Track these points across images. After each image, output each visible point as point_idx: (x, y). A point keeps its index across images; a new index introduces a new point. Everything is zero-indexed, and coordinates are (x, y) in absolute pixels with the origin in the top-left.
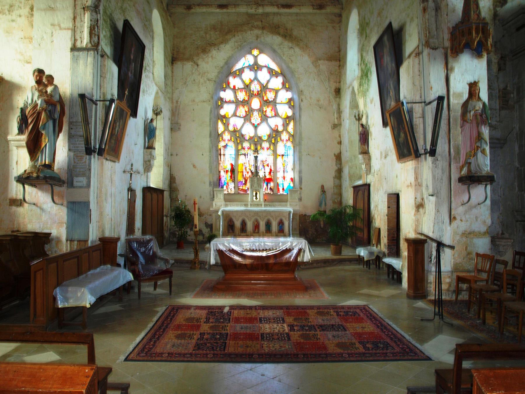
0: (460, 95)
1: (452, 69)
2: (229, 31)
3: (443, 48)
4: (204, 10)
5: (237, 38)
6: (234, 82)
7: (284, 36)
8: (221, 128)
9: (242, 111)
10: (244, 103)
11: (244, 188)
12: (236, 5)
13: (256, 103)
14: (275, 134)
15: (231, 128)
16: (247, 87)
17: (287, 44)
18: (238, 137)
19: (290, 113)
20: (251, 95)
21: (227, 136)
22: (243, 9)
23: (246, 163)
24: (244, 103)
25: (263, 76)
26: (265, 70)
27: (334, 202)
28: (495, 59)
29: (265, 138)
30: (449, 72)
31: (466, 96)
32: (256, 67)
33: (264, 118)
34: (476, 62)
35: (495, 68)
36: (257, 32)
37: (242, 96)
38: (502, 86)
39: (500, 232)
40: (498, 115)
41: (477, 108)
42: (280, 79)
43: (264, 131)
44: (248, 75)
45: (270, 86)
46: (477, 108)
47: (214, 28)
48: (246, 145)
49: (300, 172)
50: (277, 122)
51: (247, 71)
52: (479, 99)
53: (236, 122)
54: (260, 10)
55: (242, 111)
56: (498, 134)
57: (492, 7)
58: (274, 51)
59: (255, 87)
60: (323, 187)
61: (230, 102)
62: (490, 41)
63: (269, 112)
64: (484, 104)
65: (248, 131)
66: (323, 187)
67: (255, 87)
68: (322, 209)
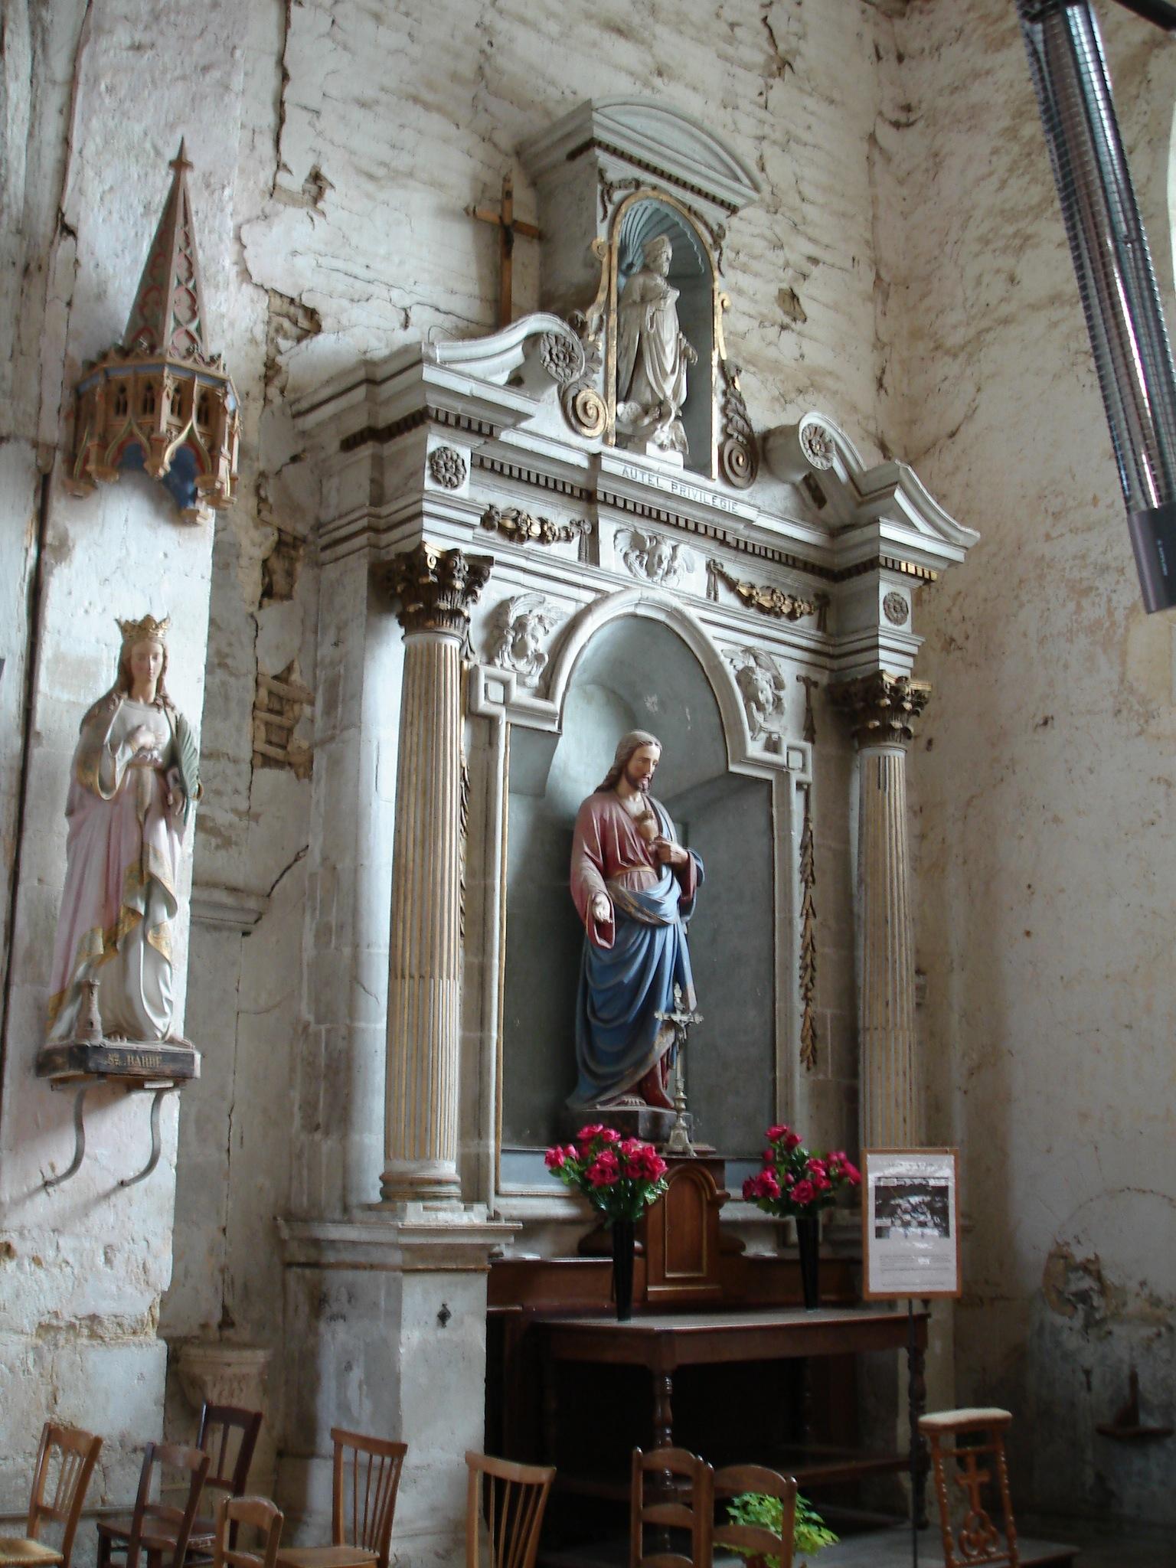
0: (84, 669)
1: (63, 550)
3: (35, 445)
28: (255, 544)
30: (47, 556)
31: (108, 677)
34: (168, 536)
35: (250, 582)
38: (272, 665)
39: (218, 1316)
40: (243, 787)
41: (145, 739)
46: (145, 739)
52: (162, 702)
56: (240, 868)
57: (260, 331)
62: (227, 465)
64: (179, 730)
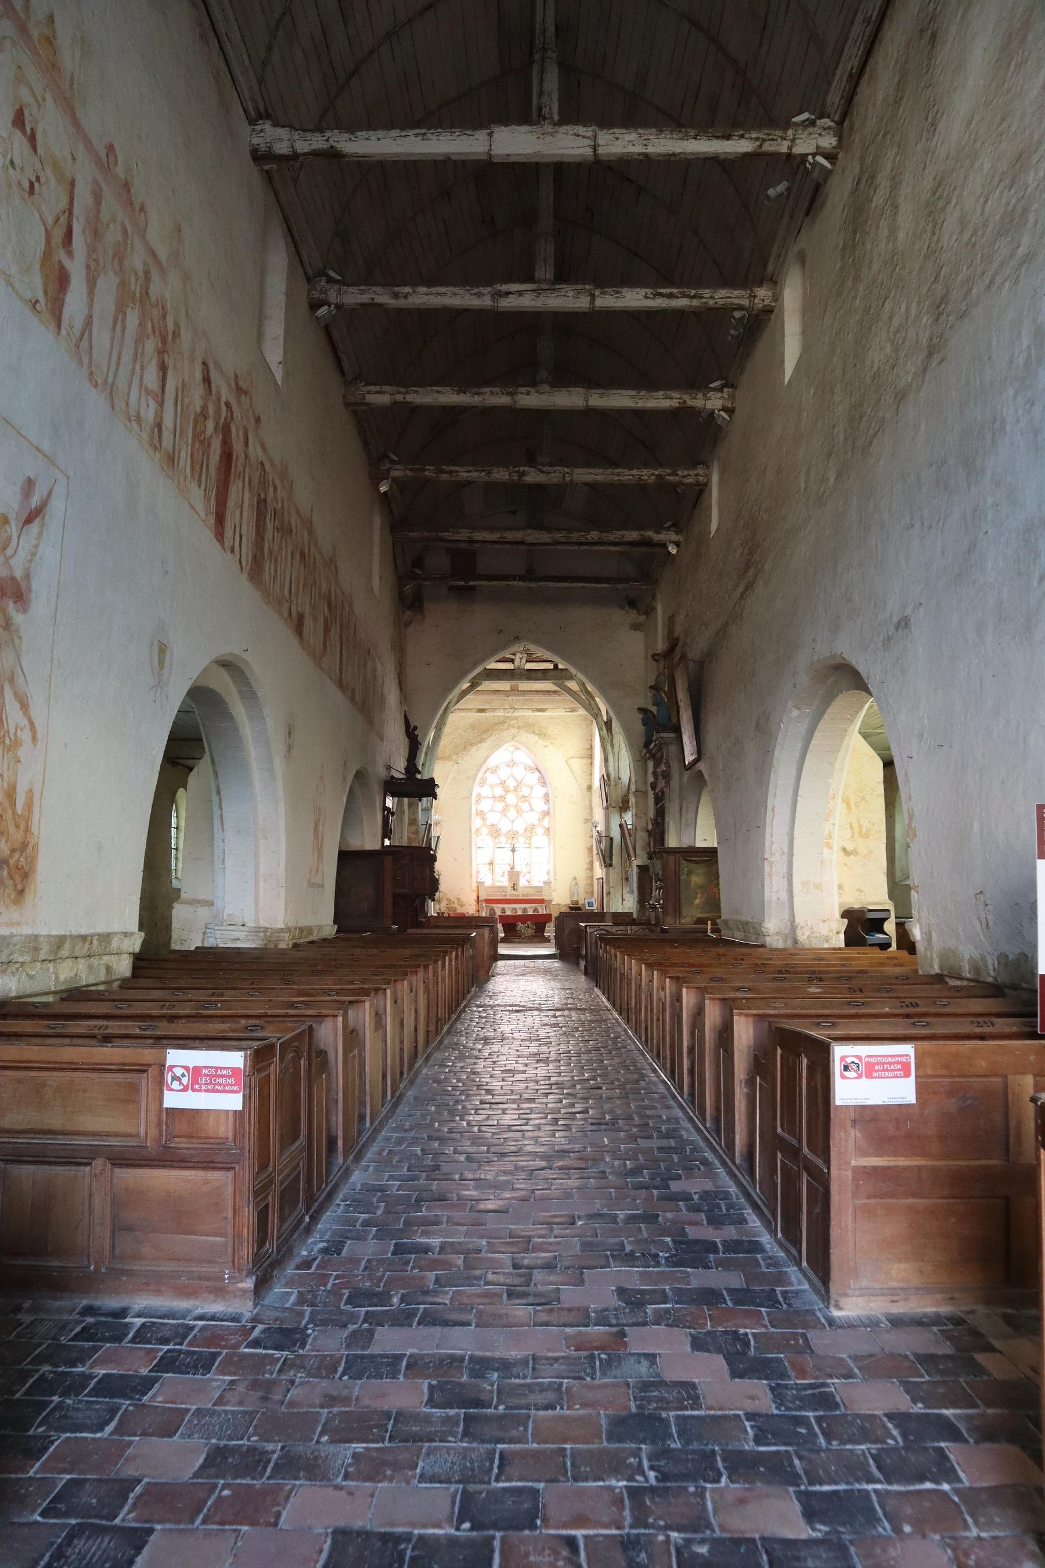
2: (486, 731)
4: (464, 714)
5: (493, 738)
6: (492, 779)
7: (539, 735)
8: (477, 822)
9: (499, 806)
10: (502, 798)
11: (502, 879)
12: (493, 710)
13: (511, 799)
14: (531, 829)
15: (489, 823)
16: (503, 783)
17: (541, 743)
18: (495, 832)
19: (545, 808)
20: (507, 791)
21: (485, 831)
22: (500, 713)
23: (503, 858)
24: (502, 798)
25: (519, 772)
26: (521, 767)
27: (586, 892)
29: (521, 831)
32: (512, 764)
33: (519, 811)
36: (513, 731)
37: (499, 791)
42: (537, 774)
43: (520, 826)
44: (504, 773)
45: (524, 781)
47: (473, 727)
48: (503, 839)
49: (555, 864)
50: (532, 818)
51: (503, 768)
53: (492, 818)
54: (516, 714)
55: (499, 806)
58: (529, 749)
59: (511, 784)
60: (575, 878)
61: (487, 797)
63: (525, 806)
65: (505, 826)
66: (575, 878)
67: (511, 784)
68: (575, 899)
